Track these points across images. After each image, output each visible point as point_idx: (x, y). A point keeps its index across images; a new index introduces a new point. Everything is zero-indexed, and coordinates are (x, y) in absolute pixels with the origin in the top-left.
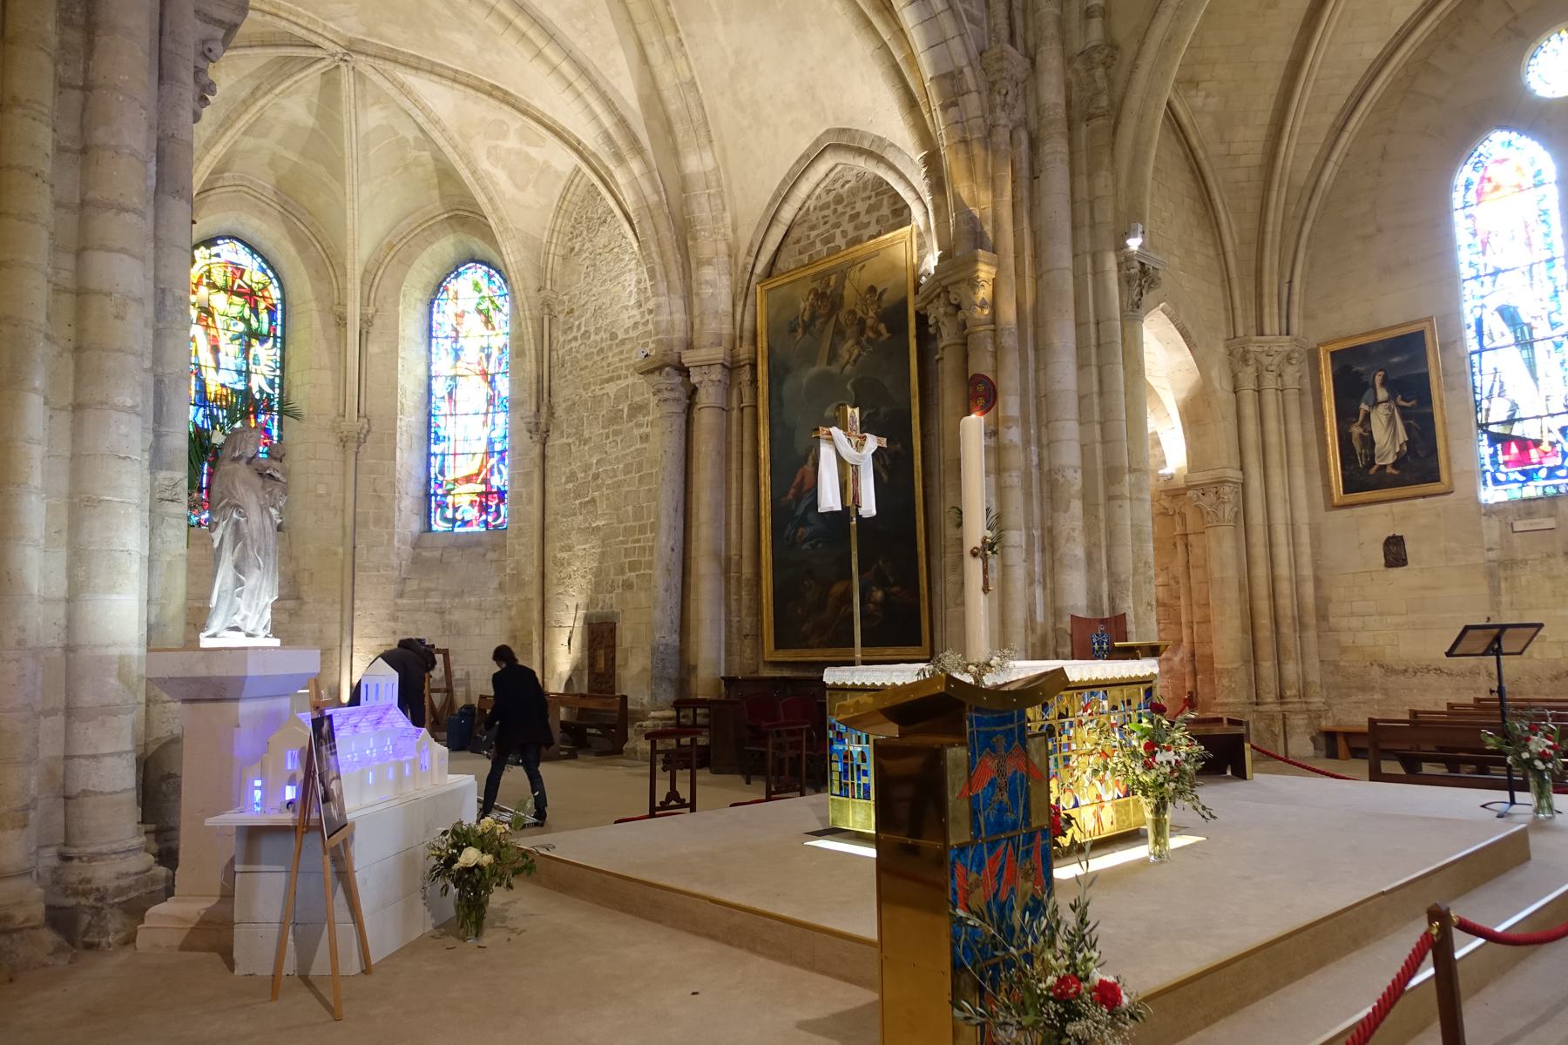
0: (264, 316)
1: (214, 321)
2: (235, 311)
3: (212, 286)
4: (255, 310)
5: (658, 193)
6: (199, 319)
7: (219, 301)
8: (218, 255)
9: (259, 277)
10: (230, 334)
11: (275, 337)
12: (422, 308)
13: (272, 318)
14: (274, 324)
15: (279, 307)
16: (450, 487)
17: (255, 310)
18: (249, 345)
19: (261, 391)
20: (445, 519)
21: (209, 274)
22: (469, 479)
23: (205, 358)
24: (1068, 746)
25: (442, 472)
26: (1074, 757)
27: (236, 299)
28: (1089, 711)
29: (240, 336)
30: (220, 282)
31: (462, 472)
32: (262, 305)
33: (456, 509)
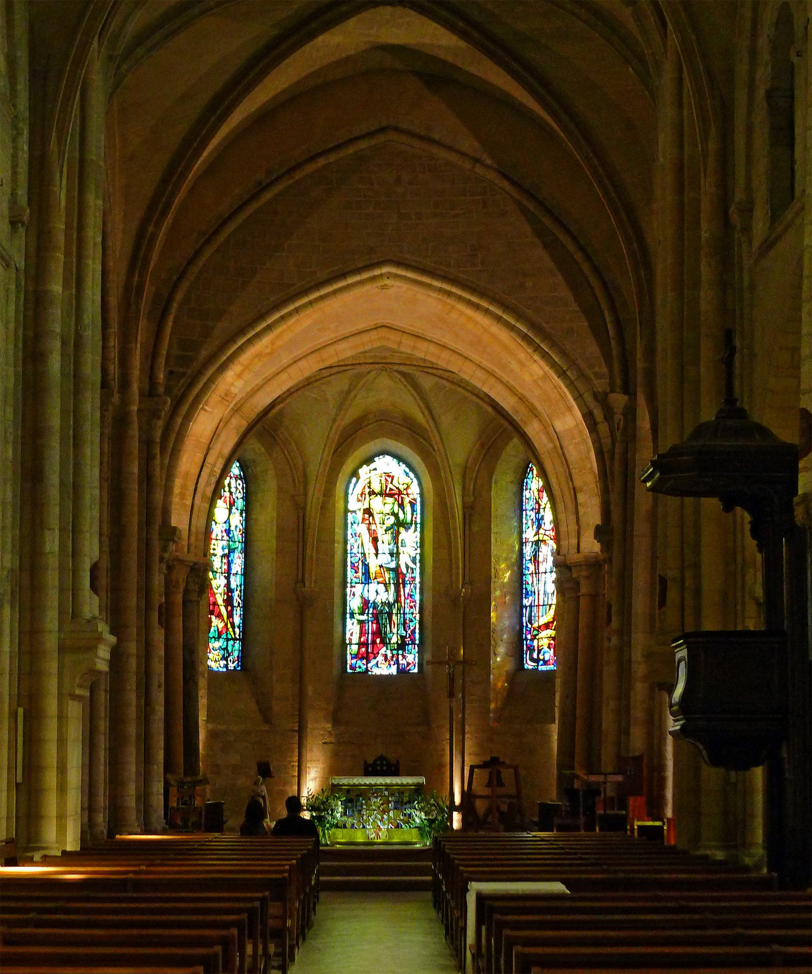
0: (408, 508)
1: (373, 519)
2: (387, 509)
3: (372, 493)
4: (401, 506)
5: (551, 440)
6: (364, 519)
7: (377, 504)
8: (375, 469)
9: (404, 479)
10: (384, 527)
11: (416, 524)
12: (513, 488)
13: (413, 511)
14: (415, 513)
15: (419, 500)
16: (535, 632)
17: (401, 506)
18: (398, 533)
19: (407, 567)
20: (532, 659)
21: (370, 483)
22: (547, 626)
23: (369, 548)
24: (362, 807)
25: (530, 621)
26: (365, 810)
27: (390, 500)
28: (375, 795)
29: (392, 527)
30: (377, 489)
31: (543, 621)
32: (407, 500)
33: (539, 651)
